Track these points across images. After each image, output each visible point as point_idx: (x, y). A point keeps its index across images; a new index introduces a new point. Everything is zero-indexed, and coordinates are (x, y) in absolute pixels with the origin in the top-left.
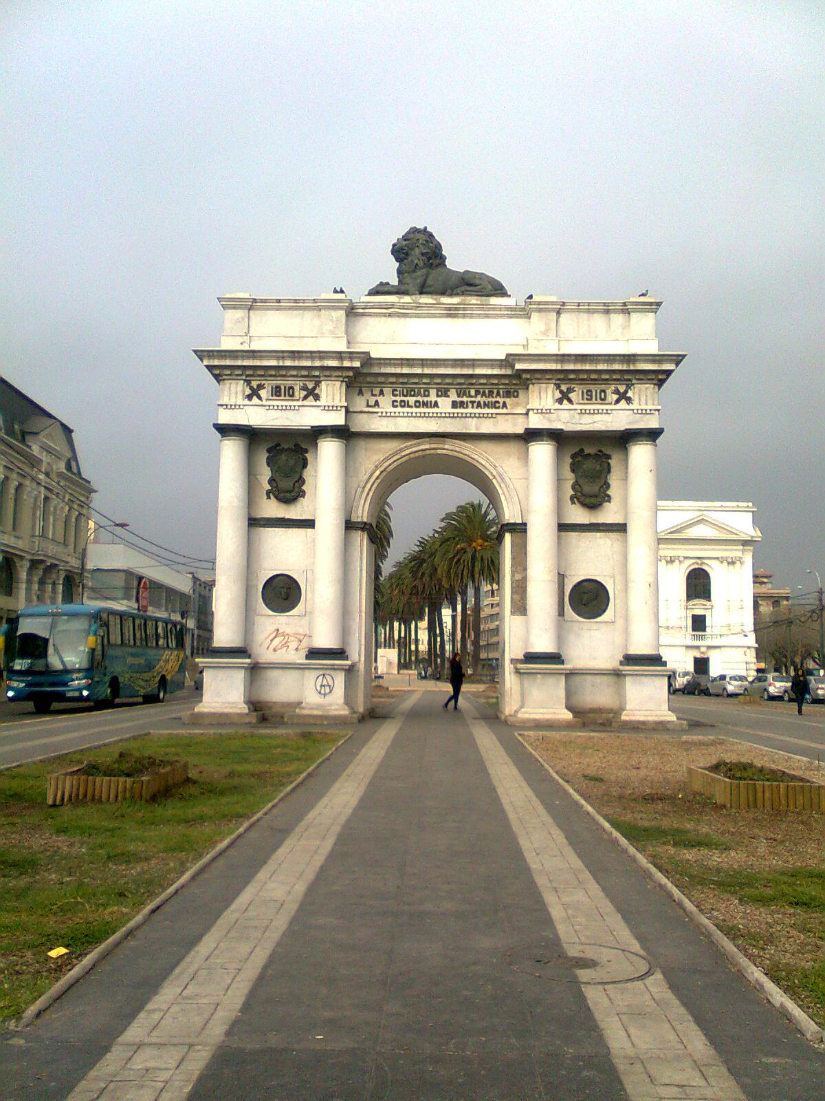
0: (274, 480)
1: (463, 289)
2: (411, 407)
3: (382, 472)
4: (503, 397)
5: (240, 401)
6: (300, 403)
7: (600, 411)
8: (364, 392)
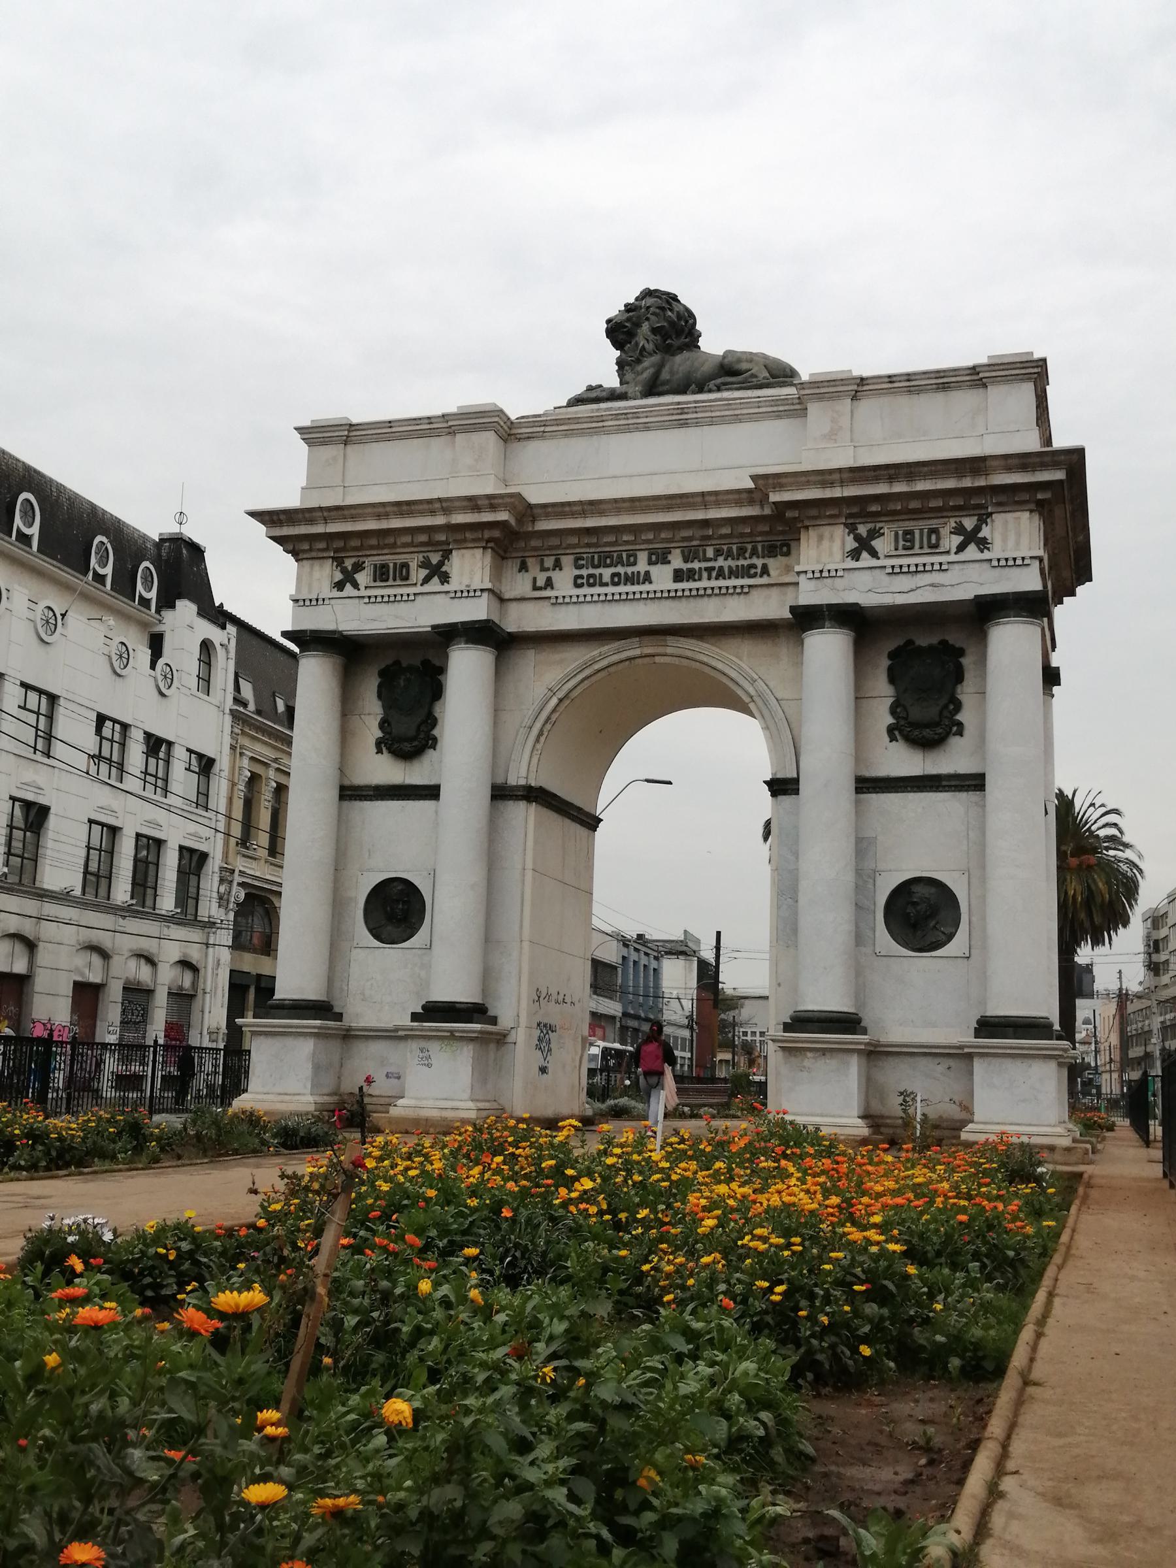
0: (389, 725)
1: (719, 381)
2: (606, 585)
3: (561, 700)
4: (763, 557)
5: (326, 591)
6: (418, 589)
7: (928, 568)
8: (529, 564)
